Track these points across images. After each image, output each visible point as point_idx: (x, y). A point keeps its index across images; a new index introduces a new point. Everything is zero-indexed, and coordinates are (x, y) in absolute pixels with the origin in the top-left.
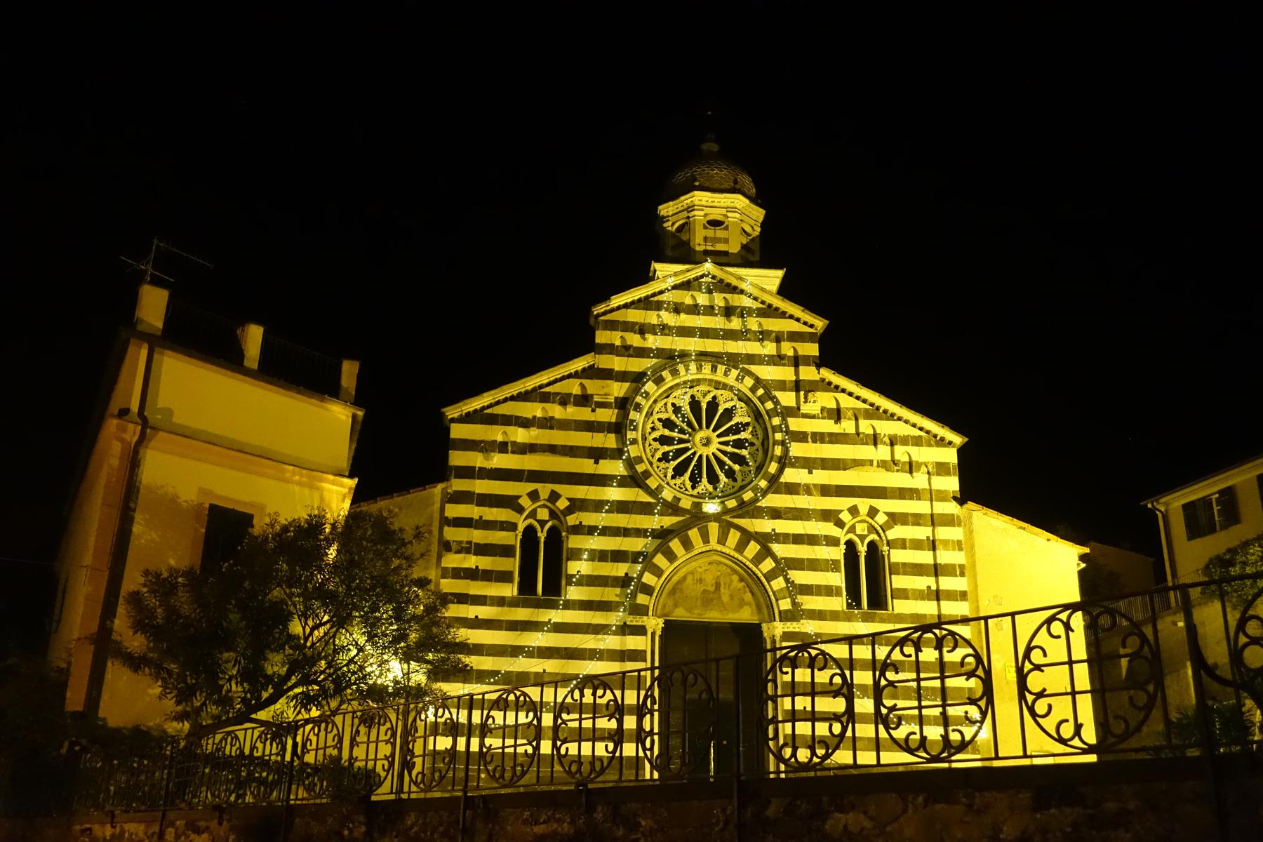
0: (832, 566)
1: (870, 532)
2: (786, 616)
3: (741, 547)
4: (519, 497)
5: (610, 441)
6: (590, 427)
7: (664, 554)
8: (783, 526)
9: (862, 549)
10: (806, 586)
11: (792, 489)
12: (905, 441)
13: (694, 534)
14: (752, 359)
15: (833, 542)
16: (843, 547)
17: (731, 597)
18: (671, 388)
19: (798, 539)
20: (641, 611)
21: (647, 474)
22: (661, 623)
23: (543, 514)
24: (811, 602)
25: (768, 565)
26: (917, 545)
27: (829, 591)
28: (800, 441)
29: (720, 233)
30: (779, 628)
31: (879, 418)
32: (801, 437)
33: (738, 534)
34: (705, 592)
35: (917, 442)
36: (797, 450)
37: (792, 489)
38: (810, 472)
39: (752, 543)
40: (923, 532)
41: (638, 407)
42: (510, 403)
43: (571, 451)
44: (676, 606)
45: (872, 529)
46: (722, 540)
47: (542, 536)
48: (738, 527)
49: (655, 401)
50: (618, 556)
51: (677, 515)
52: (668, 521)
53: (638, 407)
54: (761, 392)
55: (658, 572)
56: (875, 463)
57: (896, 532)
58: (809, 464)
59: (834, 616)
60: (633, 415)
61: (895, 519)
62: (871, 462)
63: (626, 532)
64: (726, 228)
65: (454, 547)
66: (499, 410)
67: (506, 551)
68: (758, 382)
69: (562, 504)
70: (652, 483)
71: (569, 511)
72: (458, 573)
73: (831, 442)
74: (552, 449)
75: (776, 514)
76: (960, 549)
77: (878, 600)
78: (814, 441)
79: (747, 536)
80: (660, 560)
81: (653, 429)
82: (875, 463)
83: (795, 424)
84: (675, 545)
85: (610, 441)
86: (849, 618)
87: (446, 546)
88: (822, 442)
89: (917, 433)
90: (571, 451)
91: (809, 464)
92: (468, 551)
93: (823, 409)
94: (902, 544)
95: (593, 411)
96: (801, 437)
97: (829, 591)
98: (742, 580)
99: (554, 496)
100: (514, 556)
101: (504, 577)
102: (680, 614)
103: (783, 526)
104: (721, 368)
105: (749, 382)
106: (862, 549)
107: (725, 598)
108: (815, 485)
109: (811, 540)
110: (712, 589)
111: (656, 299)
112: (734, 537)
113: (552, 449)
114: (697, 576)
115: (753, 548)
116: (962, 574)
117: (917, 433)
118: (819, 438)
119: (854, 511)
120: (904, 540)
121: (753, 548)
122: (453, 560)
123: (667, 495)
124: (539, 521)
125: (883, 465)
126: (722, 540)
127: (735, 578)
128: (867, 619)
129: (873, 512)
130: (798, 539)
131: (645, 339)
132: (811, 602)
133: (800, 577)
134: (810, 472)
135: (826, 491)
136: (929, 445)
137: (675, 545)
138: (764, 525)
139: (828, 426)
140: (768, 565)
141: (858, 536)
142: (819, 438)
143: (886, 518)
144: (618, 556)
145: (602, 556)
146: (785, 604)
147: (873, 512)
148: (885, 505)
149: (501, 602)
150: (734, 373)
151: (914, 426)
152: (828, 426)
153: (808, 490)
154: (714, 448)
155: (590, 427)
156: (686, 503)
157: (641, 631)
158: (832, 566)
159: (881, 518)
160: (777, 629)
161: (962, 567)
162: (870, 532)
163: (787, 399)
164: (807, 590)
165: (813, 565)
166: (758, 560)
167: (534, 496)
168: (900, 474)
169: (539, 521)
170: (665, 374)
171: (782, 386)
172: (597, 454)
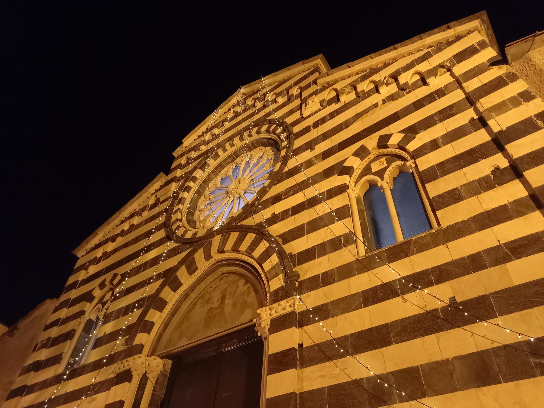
1: (389, 163)
14: (269, 114)
17: (234, 305)
18: (216, 168)
30: (266, 315)
34: (211, 309)
44: (180, 338)
59: (346, 272)
75: (277, 199)
86: (364, 265)
93: (321, 102)
110: (216, 304)
114: (206, 298)
119: (361, 153)
131: (199, 150)
146: (277, 283)
159: (395, 140)
162: (389, 163)
164: (308, 255)
167: (102, 286)
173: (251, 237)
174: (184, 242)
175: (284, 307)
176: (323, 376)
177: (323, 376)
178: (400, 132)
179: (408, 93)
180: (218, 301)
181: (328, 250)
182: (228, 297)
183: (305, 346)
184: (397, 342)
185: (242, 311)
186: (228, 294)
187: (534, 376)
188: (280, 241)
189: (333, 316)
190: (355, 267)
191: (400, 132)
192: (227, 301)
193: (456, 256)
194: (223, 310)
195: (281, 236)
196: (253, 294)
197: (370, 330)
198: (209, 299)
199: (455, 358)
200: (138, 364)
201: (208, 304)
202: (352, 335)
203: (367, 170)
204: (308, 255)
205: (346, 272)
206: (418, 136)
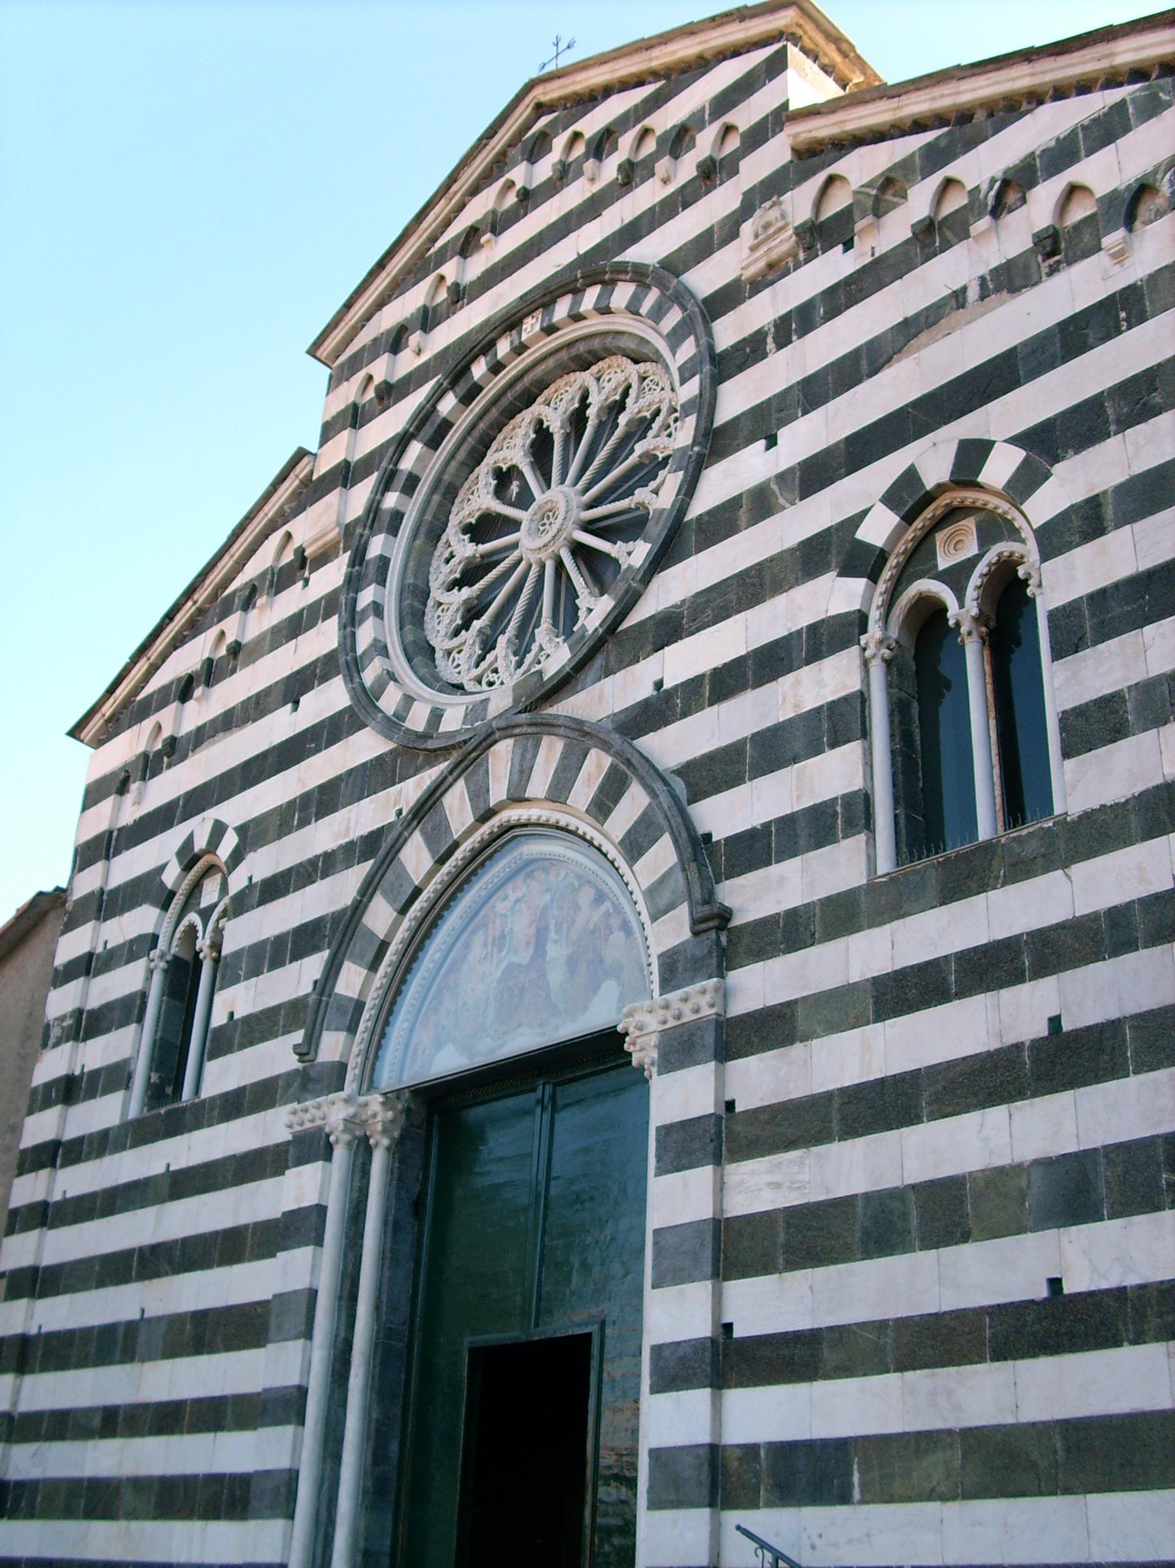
4: (161, 869)
9: (963, 610)
12: (1064, 153)
14: (632, 233)
17: (572, 963)
19: (726, 682)
24: (755, 896)
27: (816, 827)
33: (559, 745)
34: (511, 969)
35: (1106, 130)
39: (595, 755)
42: (175, 653)
43: (256, 707)
44: (439, 1045)
51: (430, 763)
52: (411, 790)
59: (840, 916)
60: (376, 546)
62: (958, 298)
75: (670, 628)
77: (1021, 793)
82: (973, 294)
97: (816, 827)
98: (600, 897)
106: (963, 610)
107: (556, 976)
108: (781, 477)
109: (769, 662)
110: (523, 957)
111: (439, 244)
125: (1009, 279)
127: (586, 897)
128: (969, 877)
130: (726, 682)
132: (755, 896)
135: (815, 475)
141: (943, 577)
142: (797, 324)
143: (1019, 454)
148: (1006, 417)
150: (591, 296)
151: (1084, 87)
159: (999, 468)
162: (986, 541)
164: (754, 849)
165: (771, 750)
168: (1059, 279)
173: (599, 766)
174: (411, 752)
176: (777, 1185)
177: (777, 1185)
178: (1016, 440)
179: (1053, 271)
180: (528, 944)
181: (802, 842)
182: (553, 935)
183: (739, 1108)
184: (933, 1117)
185: (594, 987)
186: (552, 926)
187: (1158, 1208)
188: (680, 786)
189: (805, 1038)
190: (864, 902)
191: (1016, 440)
193: (1085, 907)
194: (543, 976)
195: (686, 771)
196: (618, 937)
197: (882, 1081)
198: (503, 936)
199: (1036, 1162)
201: (500, 950)
202: (843, 1091)
204: (754, 849)
205: (840, 916)
206: (1058, 469)
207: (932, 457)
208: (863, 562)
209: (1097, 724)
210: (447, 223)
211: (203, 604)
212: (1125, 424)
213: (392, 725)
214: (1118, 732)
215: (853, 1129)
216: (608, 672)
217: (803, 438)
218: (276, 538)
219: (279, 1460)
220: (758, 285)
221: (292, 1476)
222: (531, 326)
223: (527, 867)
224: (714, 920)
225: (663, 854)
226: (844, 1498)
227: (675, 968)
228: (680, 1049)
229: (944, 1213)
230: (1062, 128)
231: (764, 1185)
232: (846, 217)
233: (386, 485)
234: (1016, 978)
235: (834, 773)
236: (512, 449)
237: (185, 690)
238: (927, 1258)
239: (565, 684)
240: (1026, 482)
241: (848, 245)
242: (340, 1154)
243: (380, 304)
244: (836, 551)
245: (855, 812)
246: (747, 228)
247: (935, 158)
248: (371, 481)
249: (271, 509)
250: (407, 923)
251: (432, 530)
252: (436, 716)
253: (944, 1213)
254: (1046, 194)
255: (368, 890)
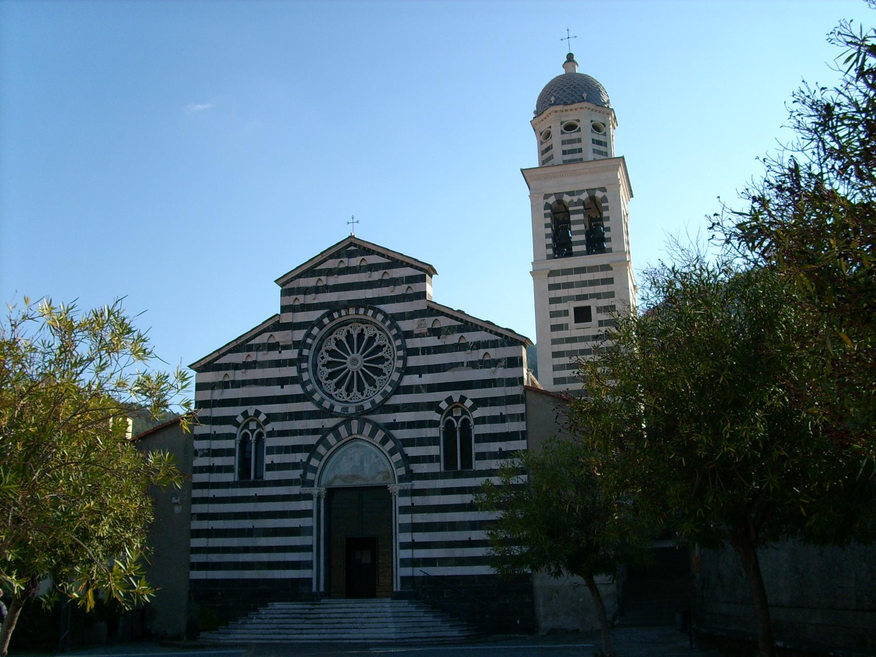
0: (434, 441)
1: (463, 414)
2: (401, 479)
3: (372, 435)
5: (292, 372)
6: (278, 364)
7: (324, 445)
8: (401, 417)
9: (457, 425)
10: (416, 457)
11: (408, 390)
13: (342, 430)
15: (433, 424)
16: (442, 426)
19: (411, 425)
20: (311, 483)
21: (314, 392)
22: (323, 490)
23: (253, 426)
24: (418, 468)
25: (390, 445)
26: (493, 420)
27: (430, 459)
28: (414, 354)
29: (574, 135)
31: (468, 331)
32: (414, 352)
35: (494, 344)
36: (412, 361)
37: (408, 390)
38: (420, 376)
40: (495, 411)
41: (309, 347)
42: (229, 355)
43: (267, 382)
45: (464, 412)
46: (360, 432)
47: (253, 438)
48: (369, 421)
49: (322, 340)
50: (296, 449)
53: (309, 347)
54: (388, 323)
55: (320, 457)
56: (465, 364)
57: (477, 414)
58: (419, 370)
59: (435, 476)
61: (479, 403)
63: (301, 432)
64: (579, 130)
65: (200, 453)
66: (222, 361)
67: (229, 452)
68: (386, 316)
69: (262, 418)
70: (317, 397)
71: (266, 422)
72: (202, 470)
73: (435, 353)
74: (256, 382)
75: (396, 409)
76: (523, 420)
77: (467, 462)
78: (423, 354)
79: (376, 427)
80: (321, 449)
81: (323, 358)
82: (465, 364)
83: (411, 343)
84: (331, 438)
85: (292, 372)
87: (196, 453)
88: (429, 353)
89: (495, 337)
90: (267, 382)
91: (419, 370)
92: (207, 455)
94: (481, 420)
95: (280, 352)
96: (414, 352)
97: (430, 459)
99: (258, 413)
100: (235, 455)
101: (229, 469)
102: (338, 483)
103: (401, 417)
104: (362, 311)
105: (380, 317)
106: (457, 425)
110: (358, 464)
111: (318, 268)
112: (368, 429)
113: (256, 382)
115: (380, 434)
116: (523, 439)
117: (495, 337)
118: (427, 351)
120: (484, 417)
121: (380, 434)
122: (199, 462)
123: (327, 404)
124: (250, 430)
125: (473, 365)
126: (360, 432)
127: (373, 456)
128: (457, 475)
129: (463, 399)
132: (418, 468)
133: (412, 451)
134: (420, 376)
136: (503, 345)
137: (331, 438)
138: (389, 418)
139: (433, 341)
140: (390, 445)
142: (427, 351)
144: (296, 449)
145: (287, 450)
147: (463, 399)
149: (227, 485)
150: (370, 312)
151: (491, 332)
152: (433, 341)
153: (417, 389)
154: (360, 365)
155: (278, 364)
156: (338, 408)
157: (308, 497)
158: (434, 441)
160: (395, 487)
161: (523, 432)
162: (463, 414)
163: (406, 325)
166: (384, 442)
168: (482, 370)
169: (250, 430)
170: (326, 321)
171: (403, 316)
172: (282, 382)
175: (406, 485)
192: (365, 465)
195: (401, 440)
200: (315, 491)
203: (450, 413)
205: (435, 476)
207: (456, 395)
208: (440, 411)
209: (481, 456)
210: (321, 263)
211: (241, 345)
212: (491, 405)
213: (319, 404)
214: (485, 459)
215: (436, 512)
216: (381, 413)
217: (428, 379)
218: (268, 334)
219: (310, 559)
220: (418, 336)
221: (312, 561)
222: (352, 311)
223: (358, 446)
224: (409, 471)
225: (398, 457)
226: (435, 566)
227: (401, 479)
228: (403, 493)
229: (453, 526)
230: (487, 339)
231: (419, 518)
232: (439, 329)
233: (308, 335)
234: (466, 493)
235: (434, 450)
236: (342, 335)
237: (236, 367)
238: (449, 533)
239: (370, 412)
240: (473, 409)
241: (439, 338)
242: (315, 499)
243: (299, 276)
244: (433, 406)
245: (436, 459)
246: (416, 320)
247: (460, 329)
248: (304, 332)
249: (265, 326)
250: (329, 453)
251: (318, 349)
252: (332, 406)
253: (453, 526)
254: (482, 352)
255: (318, 443)
